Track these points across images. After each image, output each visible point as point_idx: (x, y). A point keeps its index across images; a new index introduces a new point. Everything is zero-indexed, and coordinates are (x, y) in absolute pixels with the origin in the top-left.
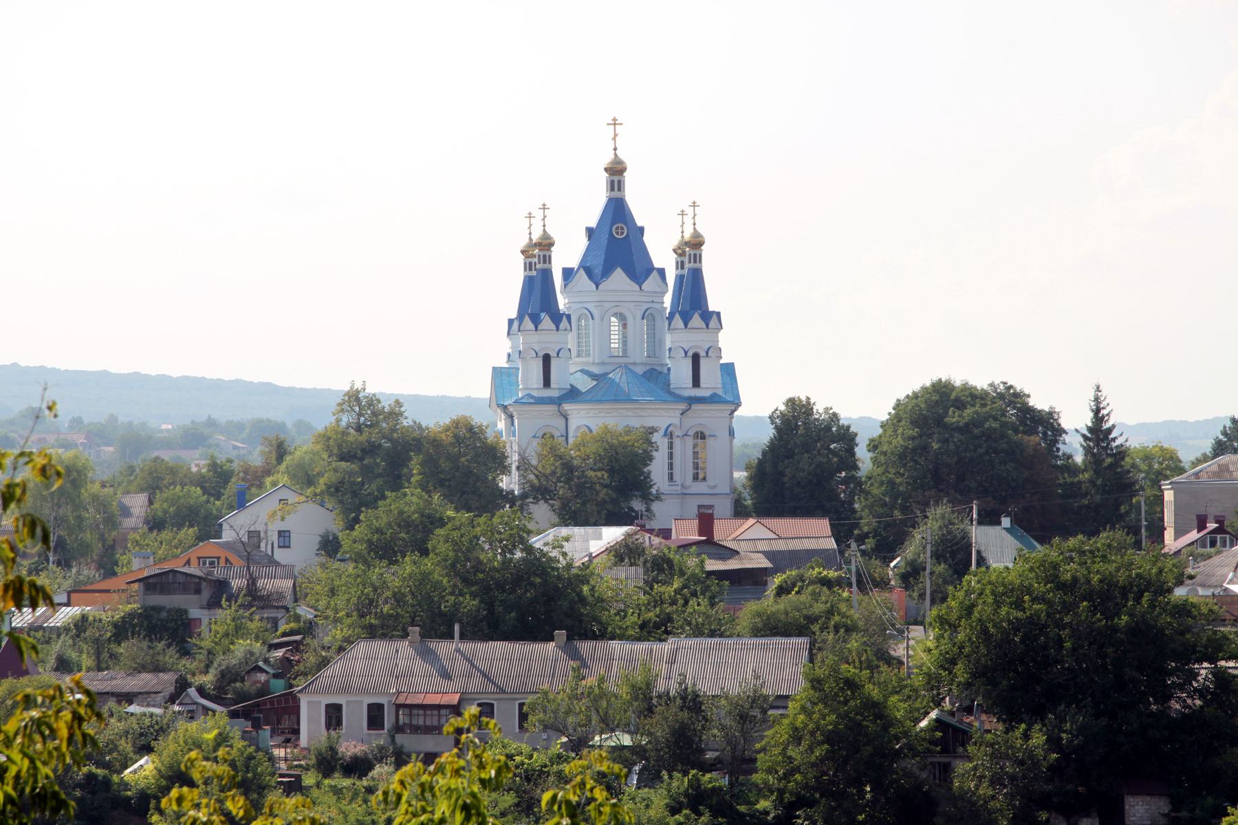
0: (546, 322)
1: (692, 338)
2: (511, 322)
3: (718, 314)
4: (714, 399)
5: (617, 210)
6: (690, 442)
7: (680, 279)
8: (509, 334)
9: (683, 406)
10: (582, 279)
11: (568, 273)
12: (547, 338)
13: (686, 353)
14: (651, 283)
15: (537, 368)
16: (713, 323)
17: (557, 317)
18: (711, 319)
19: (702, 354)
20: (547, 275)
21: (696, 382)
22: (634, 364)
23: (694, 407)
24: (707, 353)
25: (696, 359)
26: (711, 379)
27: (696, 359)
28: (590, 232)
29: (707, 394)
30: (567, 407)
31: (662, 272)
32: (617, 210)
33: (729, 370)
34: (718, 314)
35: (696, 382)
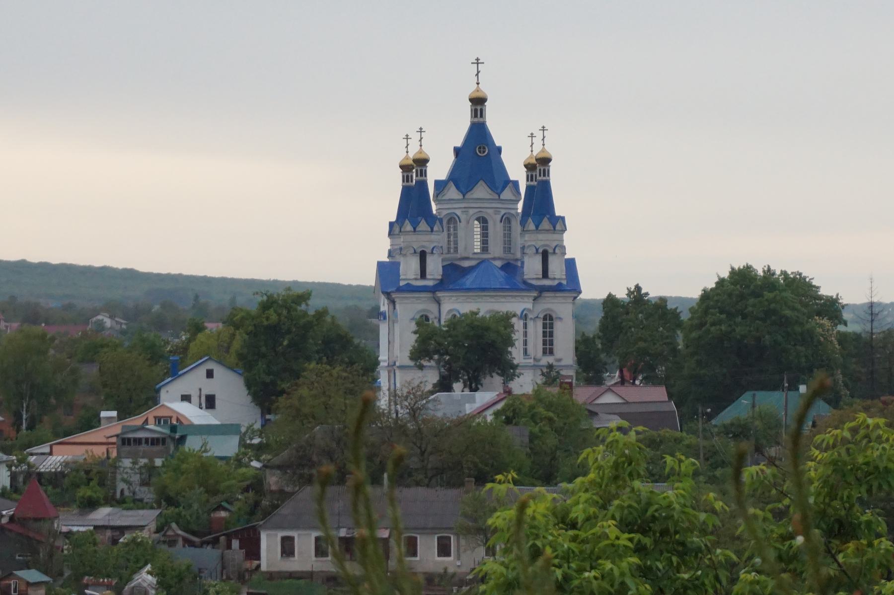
0: (423, 226)
1: (542, 240)
2: (391, 225)
3: (563, 219)
4: (558, 289)
6: (540, 324)
7: (529, 189)
10: (452, 193)
11: (440, 185)
12: (426, 239)
13: (537, 250)
14: (507, 194)
16: (558, 227)
17: (431, 220)
18: (558, 224)
19: (550, 251)
20: (423, 185)
21: (545, 274)
22: (494, 259)
24: (554, 250)
25: (545, 256)
27: (545, 256)
28: (457, 151)
30: (439, 294)
31: (516, 184)
33: (571, 265)
34: (563, 219)
35: (545, 274)
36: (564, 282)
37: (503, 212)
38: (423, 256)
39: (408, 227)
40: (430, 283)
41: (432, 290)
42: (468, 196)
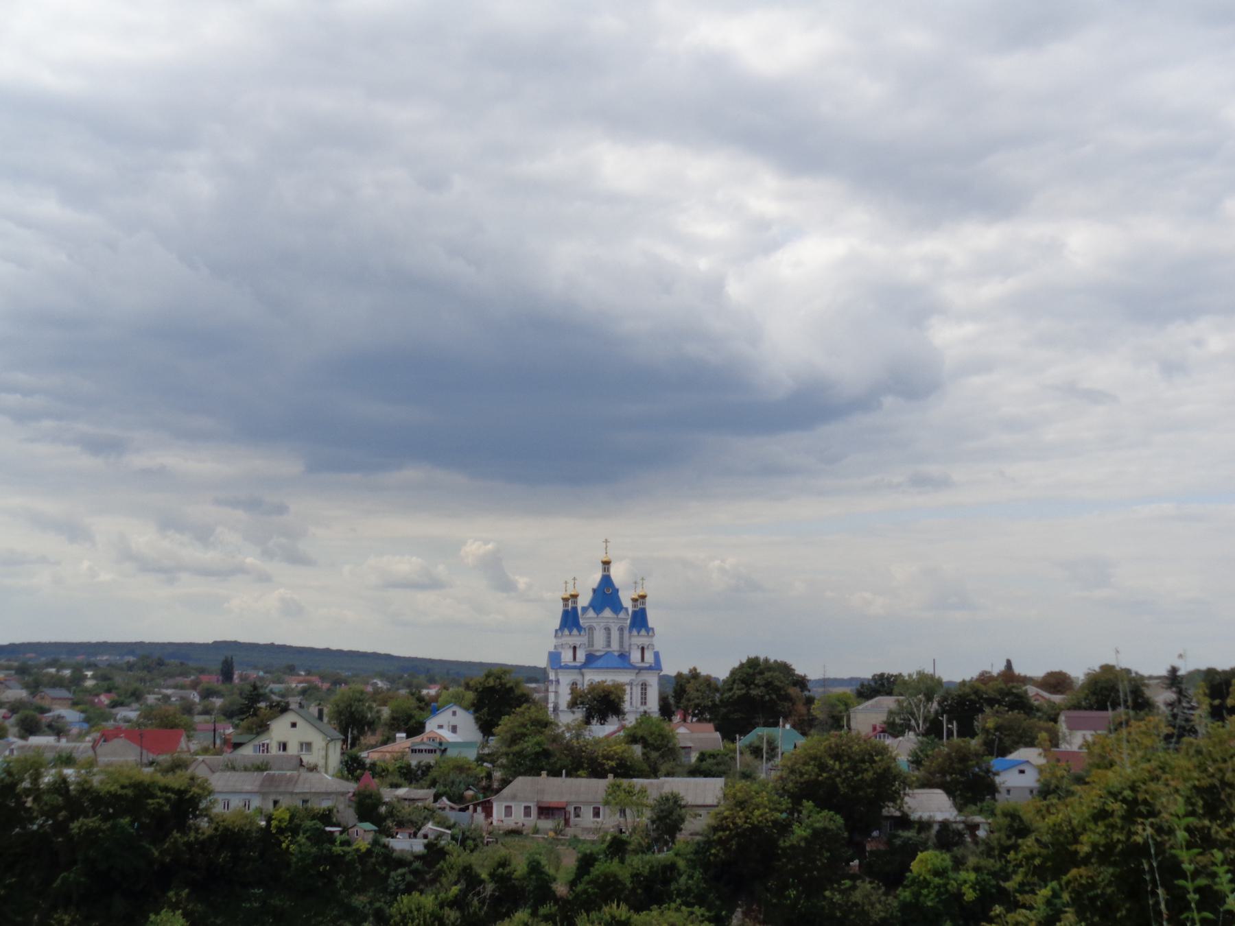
0: (575, 632)
2: (556, 631)
6: (639, 688)
8: (555, 636)
9: (637, 671)
11: (585, 609)
13: (638, 646)
15: (570, 654)
16: (651, 634)
19: (646, 647)
22: (614, 651)
23: (642, 671)
26: (649, 657)
29: (648, 665)
30: (584, 670)
33: (657, 655)
36: (653, 665)
40: (578, 664)
41: (580, 668)
42: (600, 615)
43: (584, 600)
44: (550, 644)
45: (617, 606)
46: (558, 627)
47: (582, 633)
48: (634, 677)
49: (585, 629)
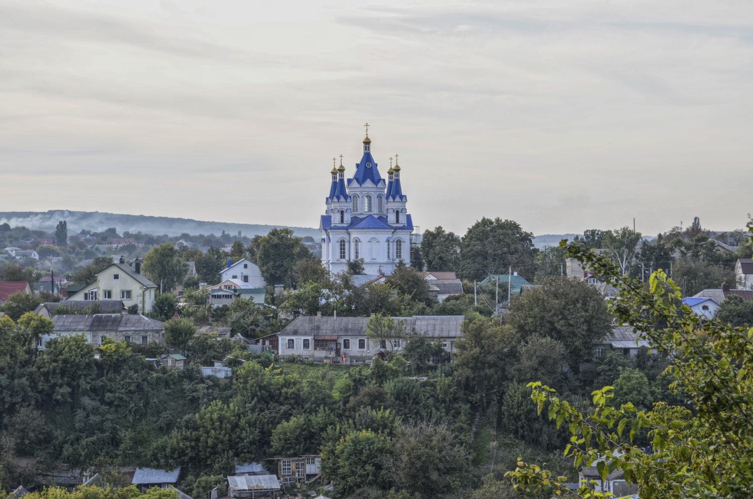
0: (342, 199)
2: (327, 199)
3: (406, 196)
5: (368, 157)
6: (395, 244)
7: (390, 183)
8: (326, 203)
10: (355, 184)
11: (349, 181)
14: (380, 185)
15: (338, 216)
16: (403, 200)
18: (403, 198)
20: (342, 181)
21: (397, 221)
26: (403, 220)
28: (358, 165)
29: (401, 225)
30: (350, 230)
31: (384, 180)
32: (368, 157)
33: (409, 217)
36: (406, 225)
37: (379, 193)
38: (342, 213)
39: (335, 200)
40: (345, 225)
41: (346, 229)
43: (350, 173)
44: (322, 209)
45: (377, 180)
46: (328, 196)
47: (348, 200)
48: (390, 236)
49: (350, 197)
